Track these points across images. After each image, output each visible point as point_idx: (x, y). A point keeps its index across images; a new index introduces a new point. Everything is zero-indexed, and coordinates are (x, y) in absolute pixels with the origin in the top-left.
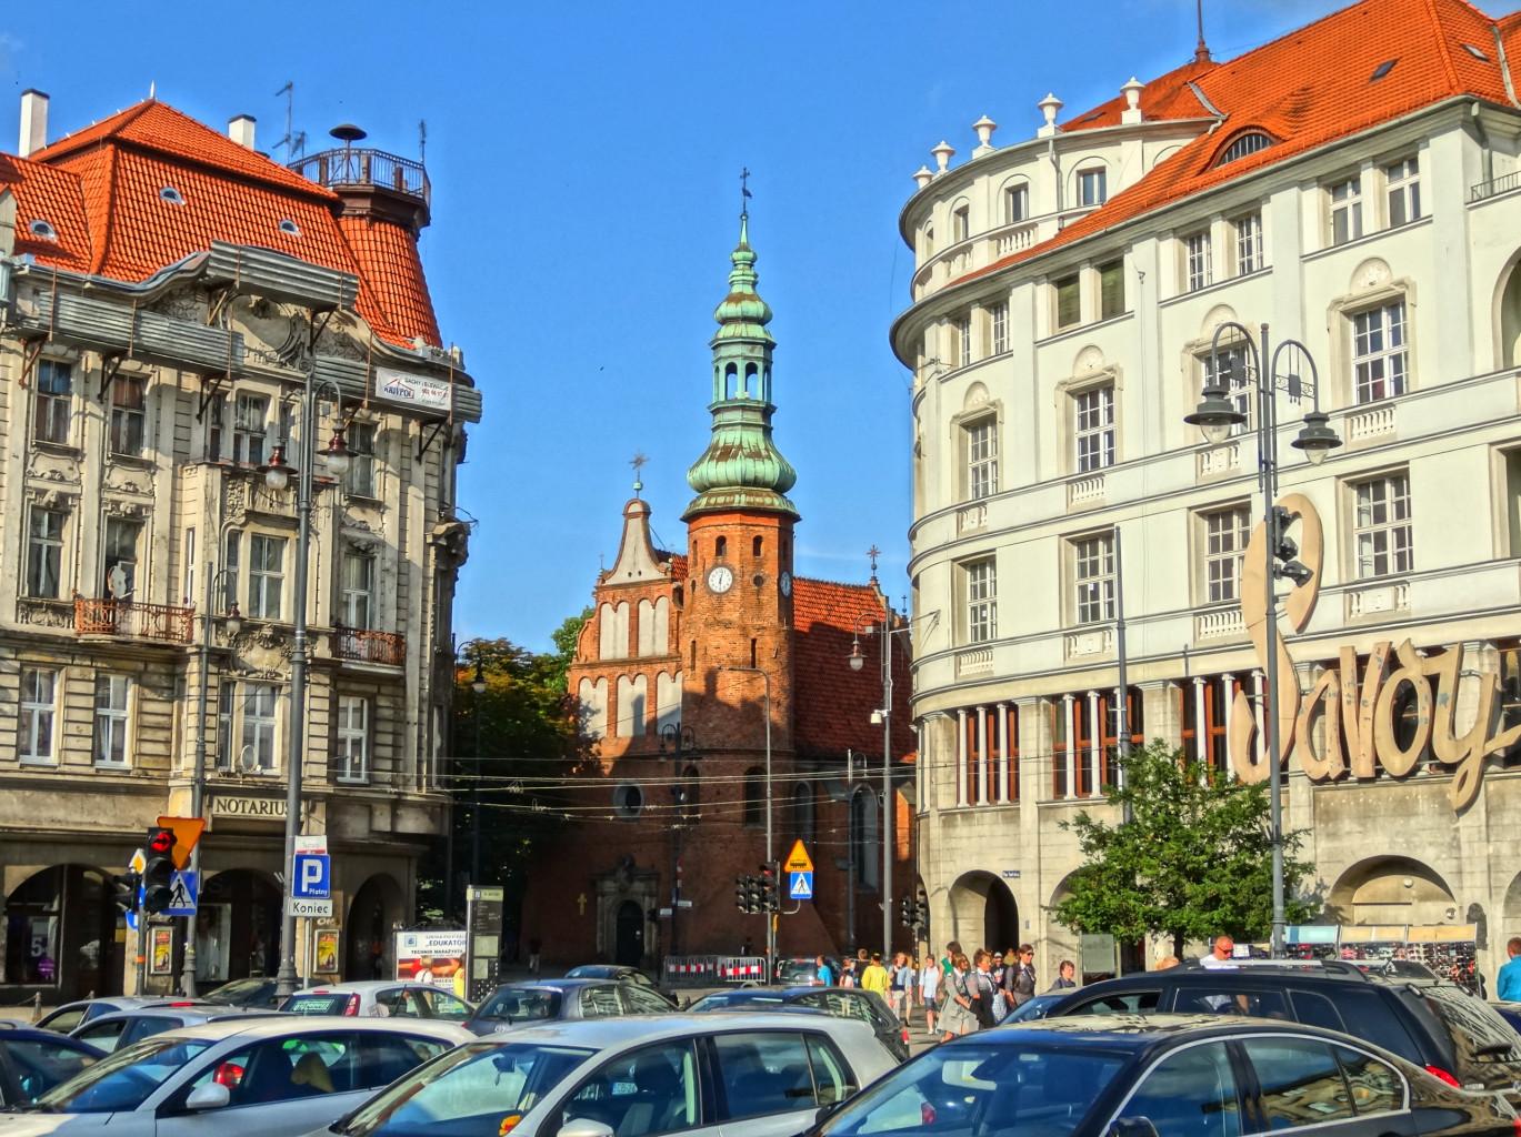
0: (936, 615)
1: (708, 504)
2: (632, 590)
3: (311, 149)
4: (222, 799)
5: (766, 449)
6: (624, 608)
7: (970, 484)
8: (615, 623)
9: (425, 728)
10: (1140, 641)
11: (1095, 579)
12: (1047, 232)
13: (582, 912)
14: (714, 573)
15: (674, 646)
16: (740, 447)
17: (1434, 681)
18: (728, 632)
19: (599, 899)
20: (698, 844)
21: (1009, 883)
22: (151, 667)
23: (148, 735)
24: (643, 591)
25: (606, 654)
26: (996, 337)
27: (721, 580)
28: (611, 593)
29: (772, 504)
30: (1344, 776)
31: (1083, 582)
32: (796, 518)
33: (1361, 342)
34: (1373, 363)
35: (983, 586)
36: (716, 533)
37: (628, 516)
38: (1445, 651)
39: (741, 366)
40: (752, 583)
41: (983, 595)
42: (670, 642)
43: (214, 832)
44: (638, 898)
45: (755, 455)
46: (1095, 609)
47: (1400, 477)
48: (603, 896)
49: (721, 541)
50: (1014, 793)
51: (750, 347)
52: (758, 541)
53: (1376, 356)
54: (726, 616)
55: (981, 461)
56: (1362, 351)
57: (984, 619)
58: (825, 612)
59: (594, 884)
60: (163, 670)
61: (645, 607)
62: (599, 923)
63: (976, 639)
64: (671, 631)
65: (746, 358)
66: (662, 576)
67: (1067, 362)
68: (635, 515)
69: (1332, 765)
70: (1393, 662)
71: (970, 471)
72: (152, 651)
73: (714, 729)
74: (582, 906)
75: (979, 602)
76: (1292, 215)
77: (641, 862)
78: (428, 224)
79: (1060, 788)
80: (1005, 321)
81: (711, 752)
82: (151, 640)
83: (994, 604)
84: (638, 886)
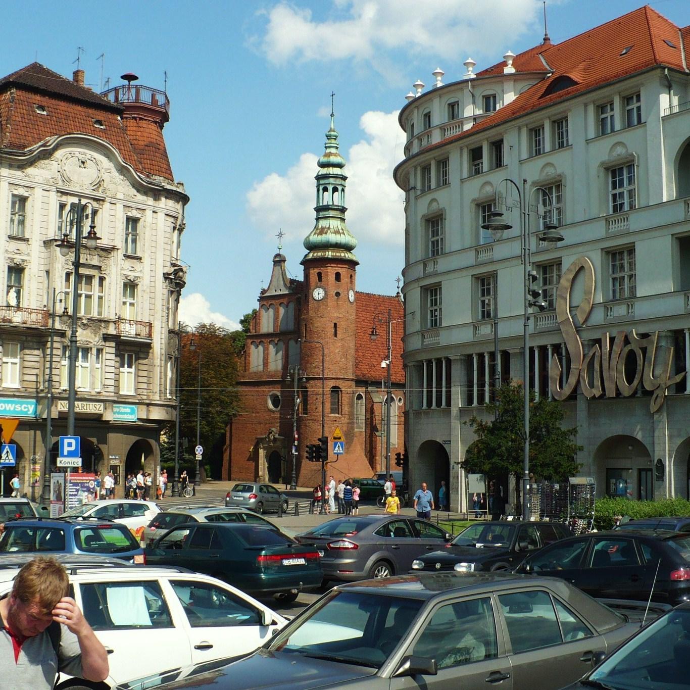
0: (413, 313)
1: (313, 256)
3: (112, 86)
4: (62, 402)
5: (342, 229)
7: (430, 249)
9: (163, 368)
10: (506, 330)
11: (488, 297)
12: (468, 126)
15: (297, 326)
16: (329, 228)
17: (644, 350)
20: (308, 424)
21: (445, 446)
22: (29, 338)
23: (27, 371)
26: (443, 177)
29: (345, 256)
30: (602, 396)
31: (483, 299)
32: (358, 264)
33: (614, 183)
34: (620, 193)
35: (436, 300)
38: (650, 336)
39: (330, 188)
41: (436, 304)
43: (60, 418)
45: (337, 232)
46: (487, 315)
47: (631, 250)
49: (320, 275)
50: (449, 403)
51: (334, 179)
53: (621, 190)
55: (435, 238)
56: (614, 188)
57: (437, 316)
58: (373, 309)
60: (34, 340)
63: (432, 326)
64: (295, 319)
65: (332, 184)
66: (291, 292)
67: (475, 189)
69: (597, 392)
70: (627, 341)
71: (430, 243)
72: (29, 331)
73: (315, 367)
75: (433, 308)
76: (581, 122)
78: (168, 121)
79: (470, 401)
80: (447, 169)
82: (28, 326)
83: (440, 309)
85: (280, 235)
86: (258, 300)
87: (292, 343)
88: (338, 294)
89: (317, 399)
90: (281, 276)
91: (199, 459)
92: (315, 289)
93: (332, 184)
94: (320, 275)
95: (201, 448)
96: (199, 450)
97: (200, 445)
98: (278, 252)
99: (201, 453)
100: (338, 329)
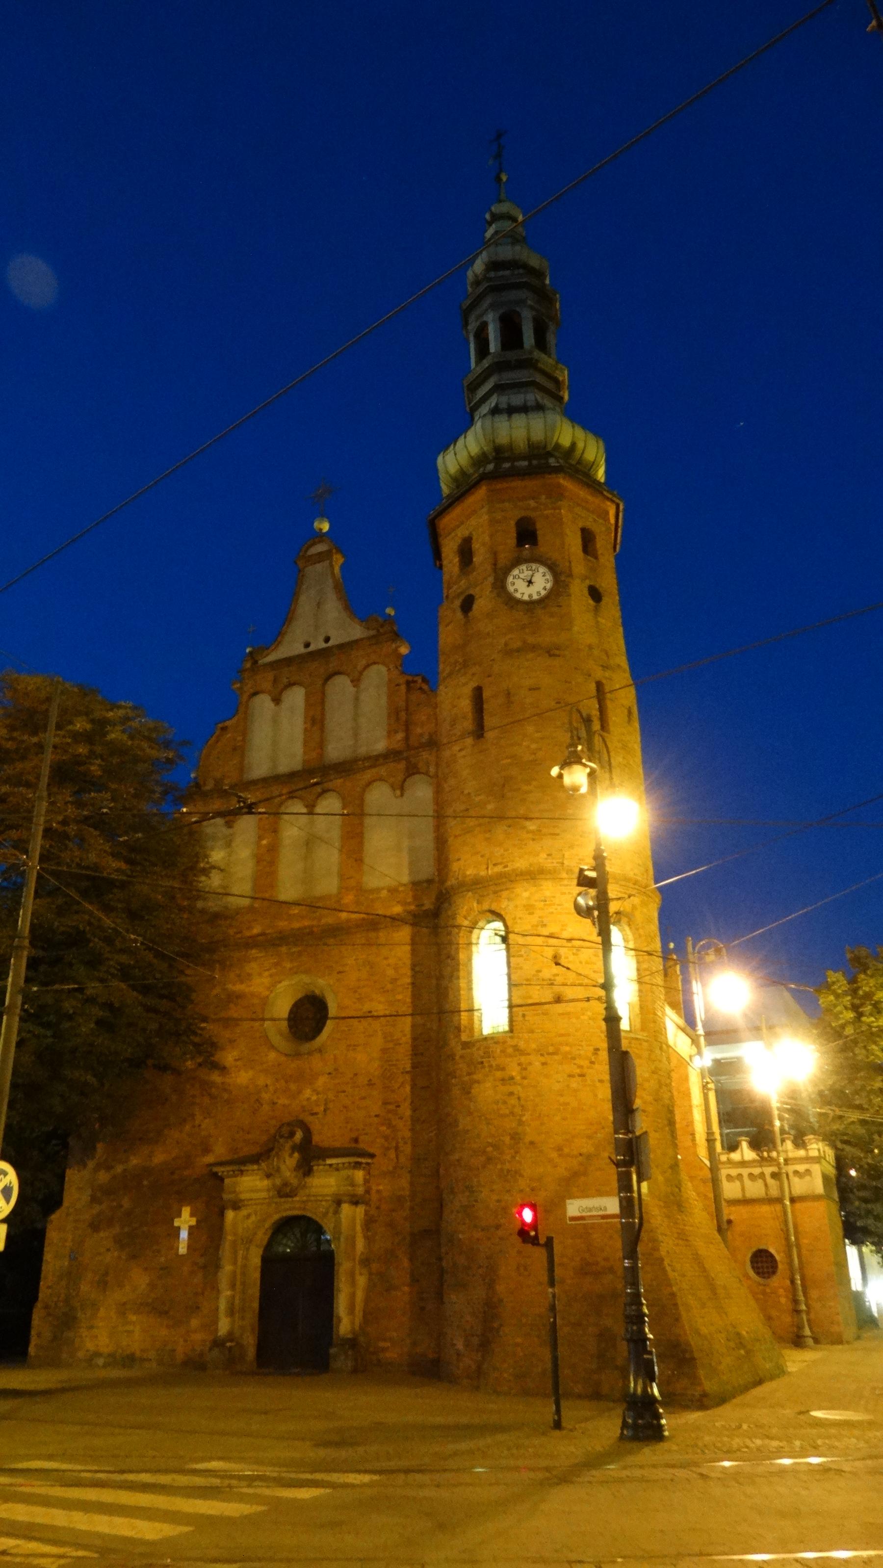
6: (296, 697)
8: (275, 721)
14: (516, 572)
15: (400, 736)
19: (230, 1215)
24: (333, 665)
27: (530, 583)
28: (270, 676)
42: (391, 733)
61: (341, 686)
62: (228, 1268)
66: (372, 633)
74: (184, 1235)
77: (326, 1134)
87: (379, 796)
100: (609, 705)
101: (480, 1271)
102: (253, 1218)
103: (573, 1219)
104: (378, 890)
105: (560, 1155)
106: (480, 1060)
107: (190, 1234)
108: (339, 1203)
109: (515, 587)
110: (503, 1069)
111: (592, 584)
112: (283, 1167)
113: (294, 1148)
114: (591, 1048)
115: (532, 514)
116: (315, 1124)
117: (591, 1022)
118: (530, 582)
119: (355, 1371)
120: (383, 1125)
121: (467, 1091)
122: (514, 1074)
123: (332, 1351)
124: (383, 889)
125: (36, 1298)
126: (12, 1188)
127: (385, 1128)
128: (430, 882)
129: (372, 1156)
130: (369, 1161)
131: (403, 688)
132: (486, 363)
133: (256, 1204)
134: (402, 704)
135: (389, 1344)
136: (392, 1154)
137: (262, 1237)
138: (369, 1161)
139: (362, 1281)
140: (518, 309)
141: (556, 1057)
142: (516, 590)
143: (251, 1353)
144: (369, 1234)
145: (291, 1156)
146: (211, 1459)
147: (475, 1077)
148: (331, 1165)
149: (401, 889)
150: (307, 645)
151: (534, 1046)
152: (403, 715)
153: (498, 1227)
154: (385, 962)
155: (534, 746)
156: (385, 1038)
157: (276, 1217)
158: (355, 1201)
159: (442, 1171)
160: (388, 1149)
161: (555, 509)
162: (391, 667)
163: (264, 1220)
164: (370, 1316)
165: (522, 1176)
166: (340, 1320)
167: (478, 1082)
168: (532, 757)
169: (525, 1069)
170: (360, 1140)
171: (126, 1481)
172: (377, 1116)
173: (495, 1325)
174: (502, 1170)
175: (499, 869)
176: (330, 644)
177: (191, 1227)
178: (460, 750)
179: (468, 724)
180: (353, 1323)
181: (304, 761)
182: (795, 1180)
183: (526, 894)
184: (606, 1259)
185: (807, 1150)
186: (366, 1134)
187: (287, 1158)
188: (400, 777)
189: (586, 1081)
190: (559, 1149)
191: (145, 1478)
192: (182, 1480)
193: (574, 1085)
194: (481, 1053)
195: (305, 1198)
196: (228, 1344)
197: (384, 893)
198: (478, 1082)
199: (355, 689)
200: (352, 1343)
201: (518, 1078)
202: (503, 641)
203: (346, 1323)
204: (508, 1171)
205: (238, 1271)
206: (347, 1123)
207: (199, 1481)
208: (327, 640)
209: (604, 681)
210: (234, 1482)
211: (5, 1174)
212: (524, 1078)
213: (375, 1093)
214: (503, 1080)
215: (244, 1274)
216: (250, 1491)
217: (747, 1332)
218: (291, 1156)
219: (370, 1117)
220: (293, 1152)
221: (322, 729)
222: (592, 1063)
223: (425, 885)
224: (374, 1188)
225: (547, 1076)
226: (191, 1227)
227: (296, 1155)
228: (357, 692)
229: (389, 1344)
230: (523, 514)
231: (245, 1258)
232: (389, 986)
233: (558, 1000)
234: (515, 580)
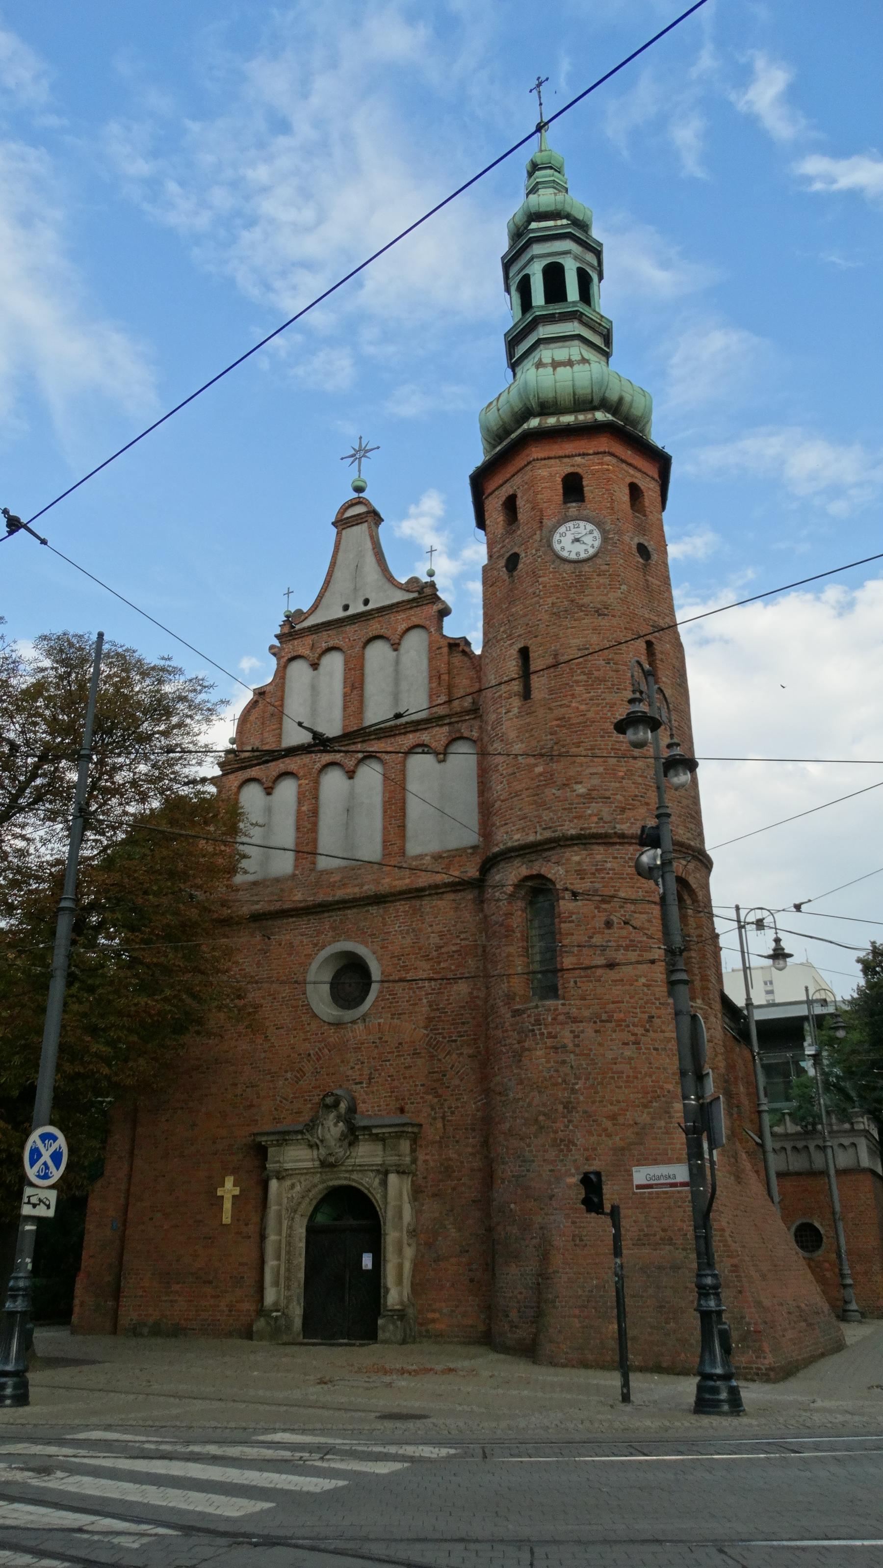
2: (349, 629)
6: (334, 663)
13: (227, 1218)
14: (562, 529)
18: (603, 622)
19: (274, 1184)
24: (375, 627)
25: (295, 737)
28: (308, 640)
36: (563, 469)
37: (342, 523)
40: (635, 546)
44: (369, 1183)
48: (278, 1179)
52: (635, 491)
54: (592, 598)
59: (261, 1152)
66: (415, 595)
68: (357, 520)
73: (589, 797)
74: (228, 1205)
81: (584, 840)
84: (367, 1153)
85: (360, 454)
86: (272, 648)
88: (643, 550)
89: (609, 924)
90: (370, 559)
91: (42, 1212)
92: (560, 524)
93: (576, 258)
94: (573, 488)
95: (61, 1142)
96: (46, 1157)
97: (52, 1123)
98: (356, 495)
99: (56, 1174)
101: (534, 1241)
102: (298, 1188)
103: (638, 1187)
104: (421, 857)
105: (614, 1125)
106: (530, 1028)
107: (233, 1204)
108: (386, 1173)
109: (562, 545)
110: (555, 1037)
111: (641, 541)
112: (328, 1136)
113: (339, 1118)
114: (646, 1016)
115: (579, 470)
116: (359, 1092)
117: (645, 989)
118: (577, 540)
119: (404, 1342)
120: (429, 1094)
121: (518, 1057)
122: (566, 1041)
123: (380, 1322)
124: (426, 855)
125: (79, 1269)
126: (61, 1154)
127: (430, 1097)
128: (475, 848)
129: (420, 1125)
130: (415, 1130)
131: (445, 650)
132: (529, 318)
133: (302, 1174)
134: (443, 668)
135: (437, 1315)
136: (440, 1125)
137: (307, 1207)
138: (415, 1130)
139: (409, 1253)
140: (560, 260)
141: (608, 1025)
142: (563, 548)
143: (298, 1323)
144: (416, 1203)
145: (336, 1125)
146: (275, 1431)
147: (526, 1045)
148: (377, 1134)
149: (444, 855)
150: (346, 608)
151: (586, 1013)
152: (445, 677)
153: (551, 1197)
154: (430, 929)
155: (583, 707)
156: (430, 1006)
157: (321, 1187)
158: (401, 1172)
159: (491, 1140)
160: (435, 1119)
161: (602, 464)
162: (432, 630)
163: (309, 1191)
164: (417, 1288)
165: (576, 1145)
166: (387, 1291)
167: (529, 1050)
168: (581, 719)
169: (578, 1037)
170: (406, 1109)
171: (192, 1453)
172: (423, 1085)
173: (550, 1296)
174: (555, 1140)
175: (548, 834)
176: (370, 606)
177: (234, 1196)
178: (506, 713)
179: (516, 686)
180: (400, 1294)
181: (345, 727)
182: (840, 1153)
183: (577, 858)
184: (664, 1230)
185: (852, 1124)
186: (412, 1103)
187: (332, 1128)
188: (444, 741)
189: (640, 1049)
190: (613, 1117)
191: (213, 1449)
192: (251, 1452)
193: (628, 1053)
194: (532, 1020)
195: (351, 1168)
196: (274, 1314)
197: (428, 858)
198: (529, 1050)
199: (395, 653)
200: (401, 1315)
201: (571, 1045)
202: (550, 601)
203: (395, 1295)
204: (562, 1140)
205: (284, 1241)
206: (392, 1092)
207: (269, 1453)
208: (366, 602)
209: (653, 640)
210: (306, 1455)
211: (55, 1138)
212: (578, 1046)
213: (419, 1062)
214: (555, 1048)
215: (289, 1244)
216: (325, 1465)
217: (806, 1305)
218: (336, 1125)
219: (416, 1086)
220: (338, 1122)
221: (362, 696)
222: (647, 1031)
223: (470, 851)
224: (421, 1157)
225: (600, 1044)
226: (234, 1196)
227: (341, 1124)
228: (397, 656)
229: (437, 1315)
230: (570, 470)
231: (290, 1227)
232: (435, 954)
233: (611, 966)
234: (562, 538)
